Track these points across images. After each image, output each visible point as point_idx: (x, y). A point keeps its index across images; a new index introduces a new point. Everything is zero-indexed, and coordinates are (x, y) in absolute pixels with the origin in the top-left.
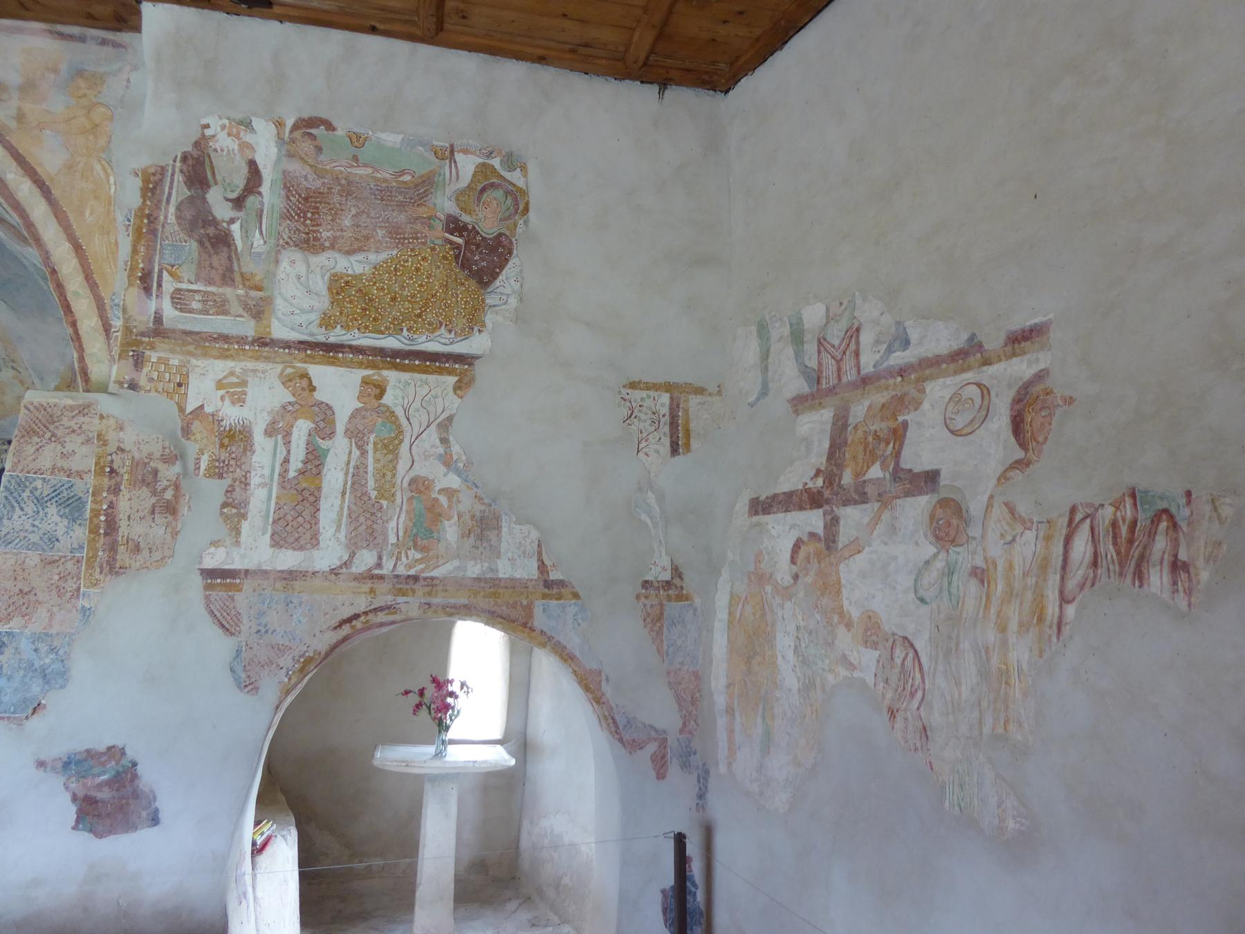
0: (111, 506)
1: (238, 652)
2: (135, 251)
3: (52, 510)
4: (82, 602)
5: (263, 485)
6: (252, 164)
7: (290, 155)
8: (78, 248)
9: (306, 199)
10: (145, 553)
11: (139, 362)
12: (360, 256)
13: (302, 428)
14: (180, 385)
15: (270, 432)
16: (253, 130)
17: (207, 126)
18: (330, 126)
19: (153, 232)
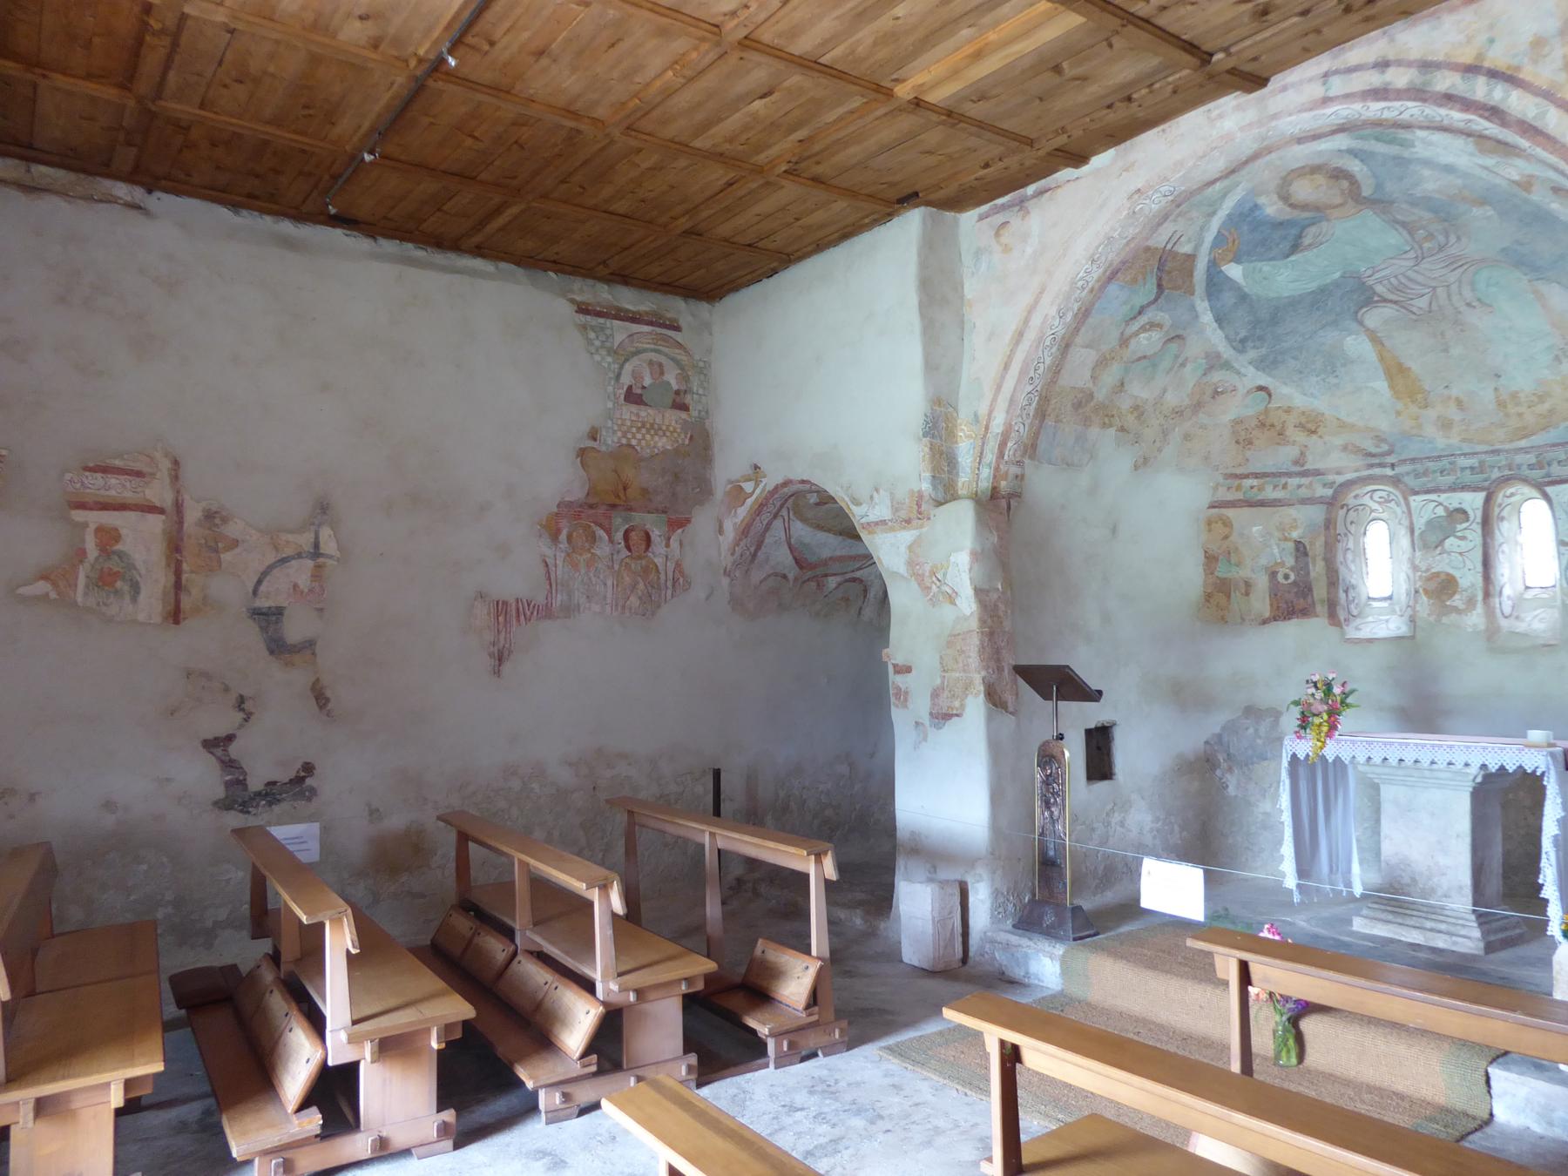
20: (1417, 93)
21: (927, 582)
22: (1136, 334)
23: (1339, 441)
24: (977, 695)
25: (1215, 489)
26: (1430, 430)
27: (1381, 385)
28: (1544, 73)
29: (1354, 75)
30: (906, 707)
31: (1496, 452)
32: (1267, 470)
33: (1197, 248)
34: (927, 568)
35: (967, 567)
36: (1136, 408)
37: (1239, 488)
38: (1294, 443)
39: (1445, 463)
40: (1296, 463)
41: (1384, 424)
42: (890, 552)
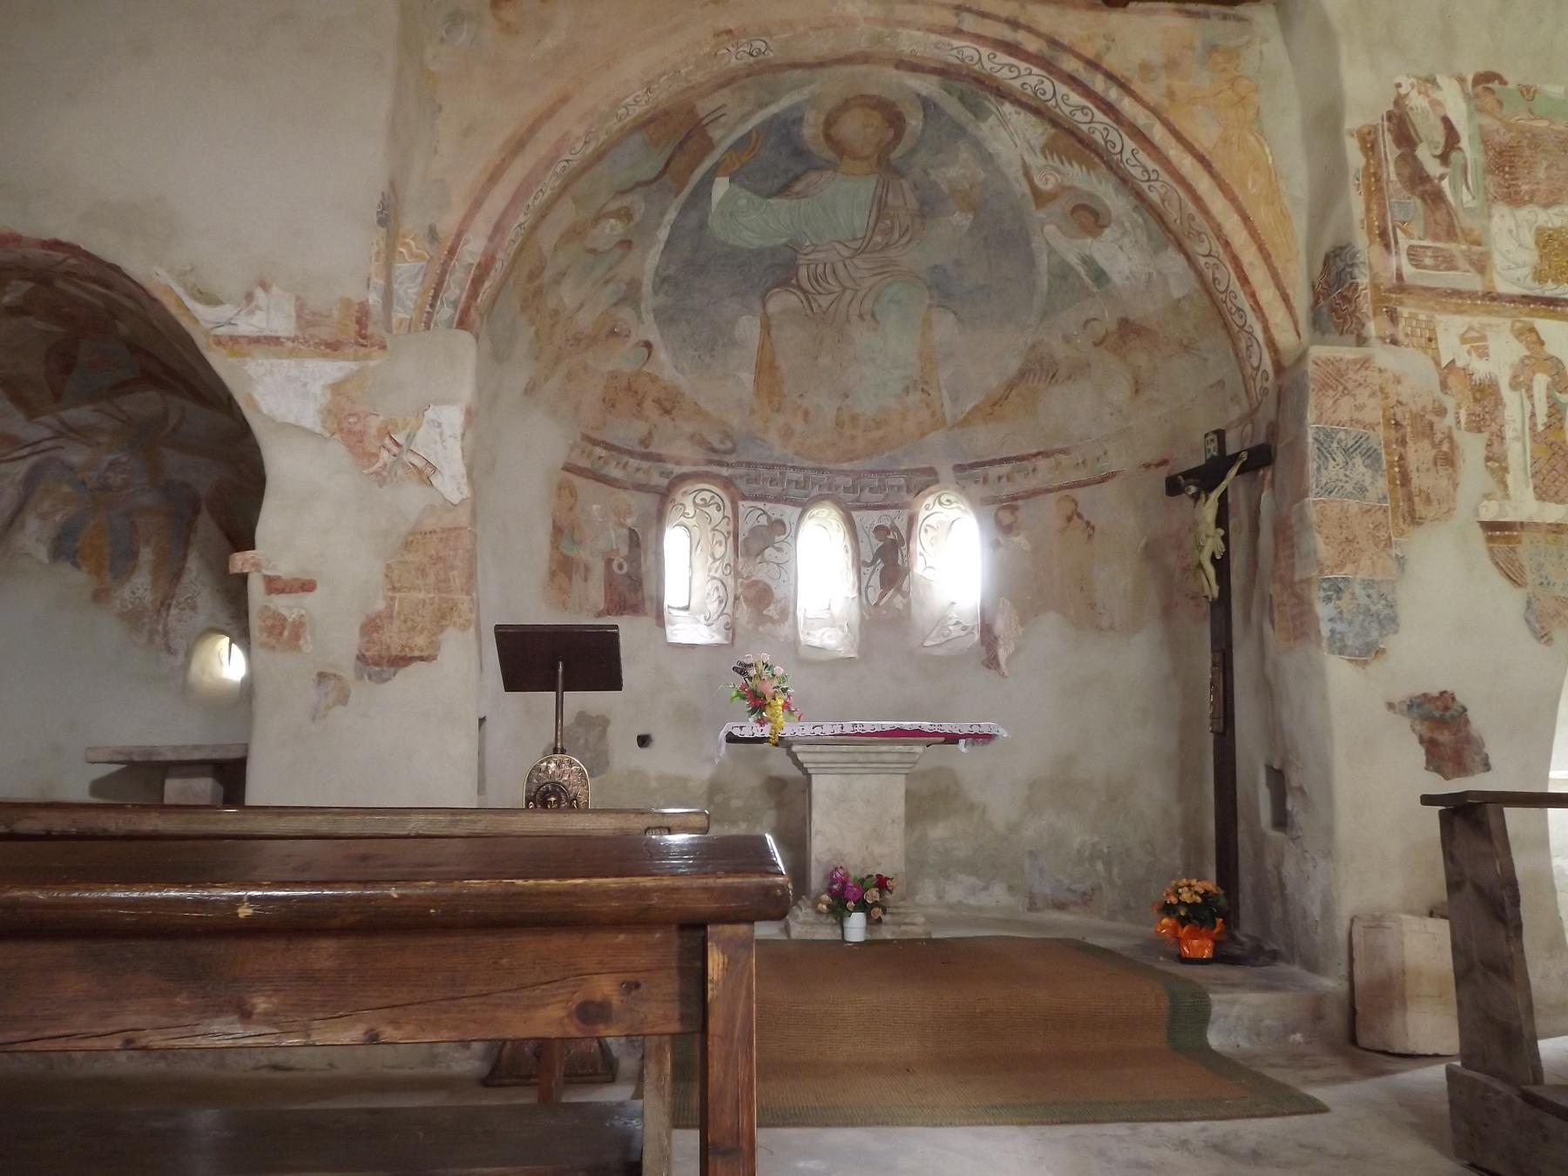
0: (1401, 458)
1: (1529, 603)
2: (1368, 210)
3: (1358, 460)
4: (1394, 551)
5: (1516, 439)
6: (1446, 121)
7: (1480, 110)
8: (1246, 219)
9: (1500, 153)
10: (1435, 503)
11: (1393, 317)
12: (1556, 210)
13: (1541, 381)
14: (1430, 340)
15: (1515, 385)
16: (1439, 88)
17: (1399, 86)
18: (1503, 82)
19: (1380, 189)
20: (1048, 65)
21: (371, 445)
22: (609, 216)
23: (688, 428)
24: (464, 628)
25: (572, 448)
26: (773, 437)
27: (748, 377)
28: (1152, 94)
29: (987, 21)
30: (297, 648)
31: (821, 470)
32: (616, 443)
33: (723, 138)
34: (374, 424)
35: (458, 431)
36: (556, 313)
37: (590, 455)
38: (647, 419)
39: (777, 473)
40: (644, 442)
41: (735, 420)
42: (281, 396)
